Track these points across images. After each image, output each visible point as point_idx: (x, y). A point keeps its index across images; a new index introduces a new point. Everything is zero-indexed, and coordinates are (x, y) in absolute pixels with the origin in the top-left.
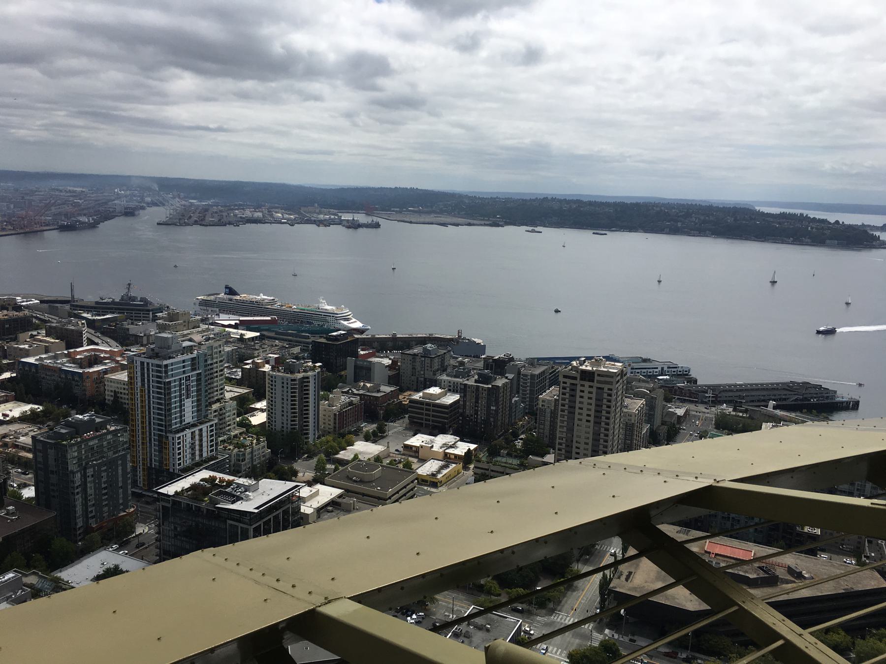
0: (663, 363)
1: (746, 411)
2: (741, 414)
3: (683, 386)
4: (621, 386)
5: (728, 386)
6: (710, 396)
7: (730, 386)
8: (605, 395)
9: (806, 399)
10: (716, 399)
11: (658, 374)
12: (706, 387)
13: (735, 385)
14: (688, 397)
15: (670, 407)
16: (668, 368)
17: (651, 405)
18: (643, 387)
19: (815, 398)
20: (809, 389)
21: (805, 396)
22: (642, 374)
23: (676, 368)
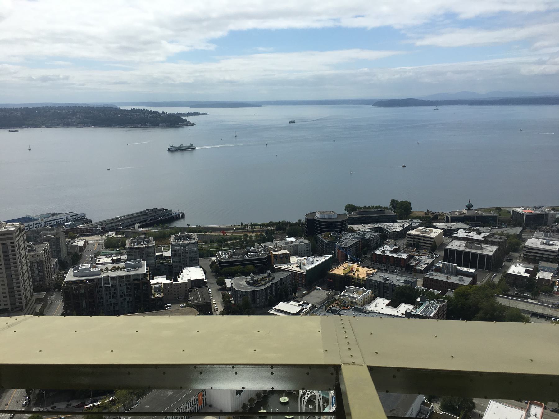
0: (66, 214)
1: (123, 233)
2: (120, 236)
3: (81, 227)
4: (22, 238)
5: (110, 220)
6: (100, 229)
7: (111, 220)
8: (9, 248)
9: (157, 218)
10: (104, 230)
11: (64, 222)
12: (96, 224)
13: (115, 219)
14: (85, 233)
15: (74, 242)
16: (70, 217)
17: (55, 245)
18: (49, 234)
19: (162, 216)
20: (157, 212)
21: (156, 216)
22: (49, 225)
23: (76, 215)
